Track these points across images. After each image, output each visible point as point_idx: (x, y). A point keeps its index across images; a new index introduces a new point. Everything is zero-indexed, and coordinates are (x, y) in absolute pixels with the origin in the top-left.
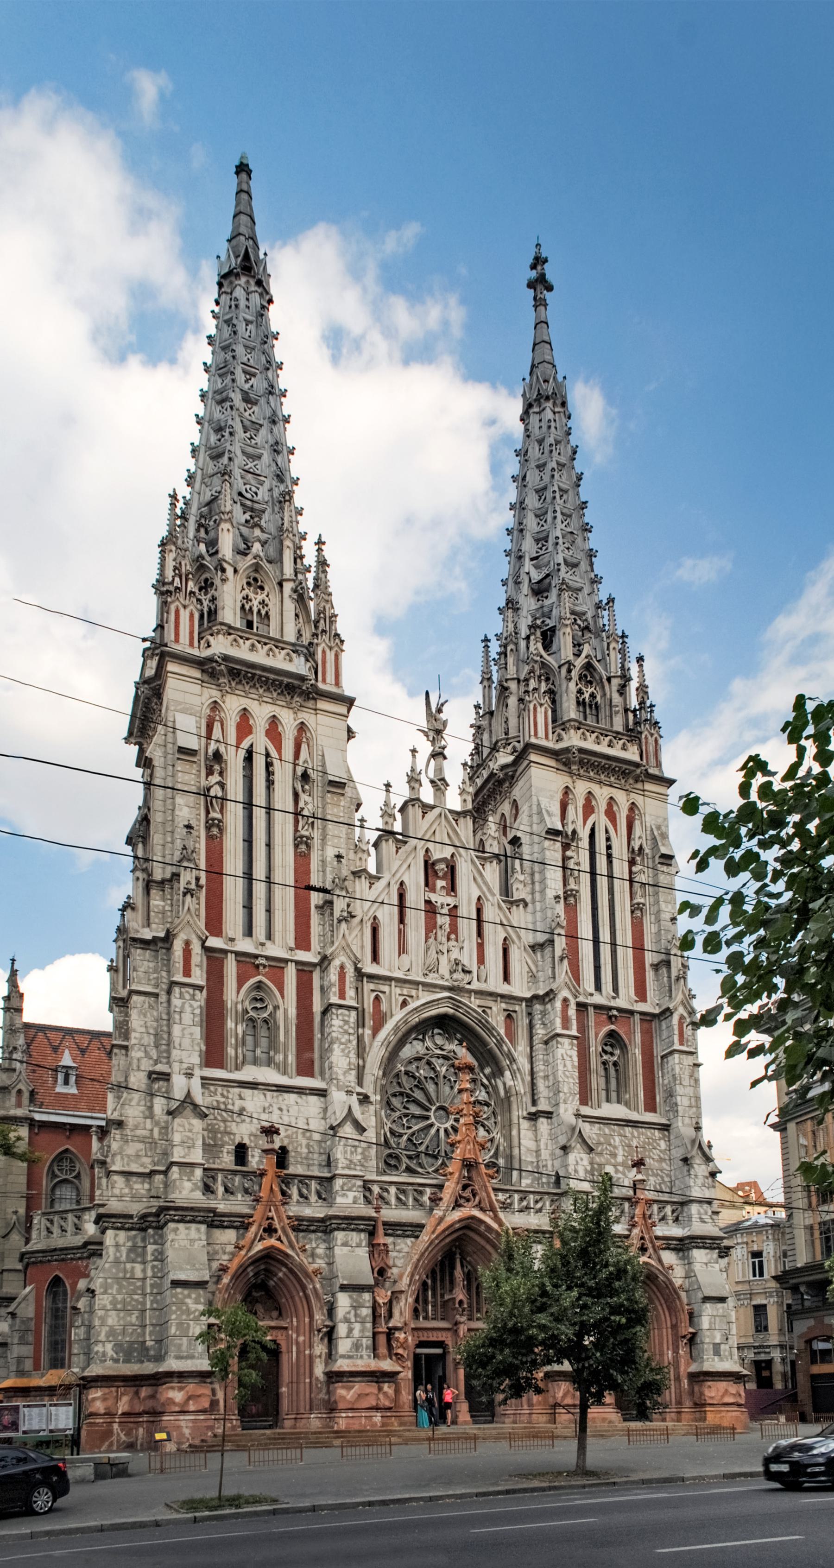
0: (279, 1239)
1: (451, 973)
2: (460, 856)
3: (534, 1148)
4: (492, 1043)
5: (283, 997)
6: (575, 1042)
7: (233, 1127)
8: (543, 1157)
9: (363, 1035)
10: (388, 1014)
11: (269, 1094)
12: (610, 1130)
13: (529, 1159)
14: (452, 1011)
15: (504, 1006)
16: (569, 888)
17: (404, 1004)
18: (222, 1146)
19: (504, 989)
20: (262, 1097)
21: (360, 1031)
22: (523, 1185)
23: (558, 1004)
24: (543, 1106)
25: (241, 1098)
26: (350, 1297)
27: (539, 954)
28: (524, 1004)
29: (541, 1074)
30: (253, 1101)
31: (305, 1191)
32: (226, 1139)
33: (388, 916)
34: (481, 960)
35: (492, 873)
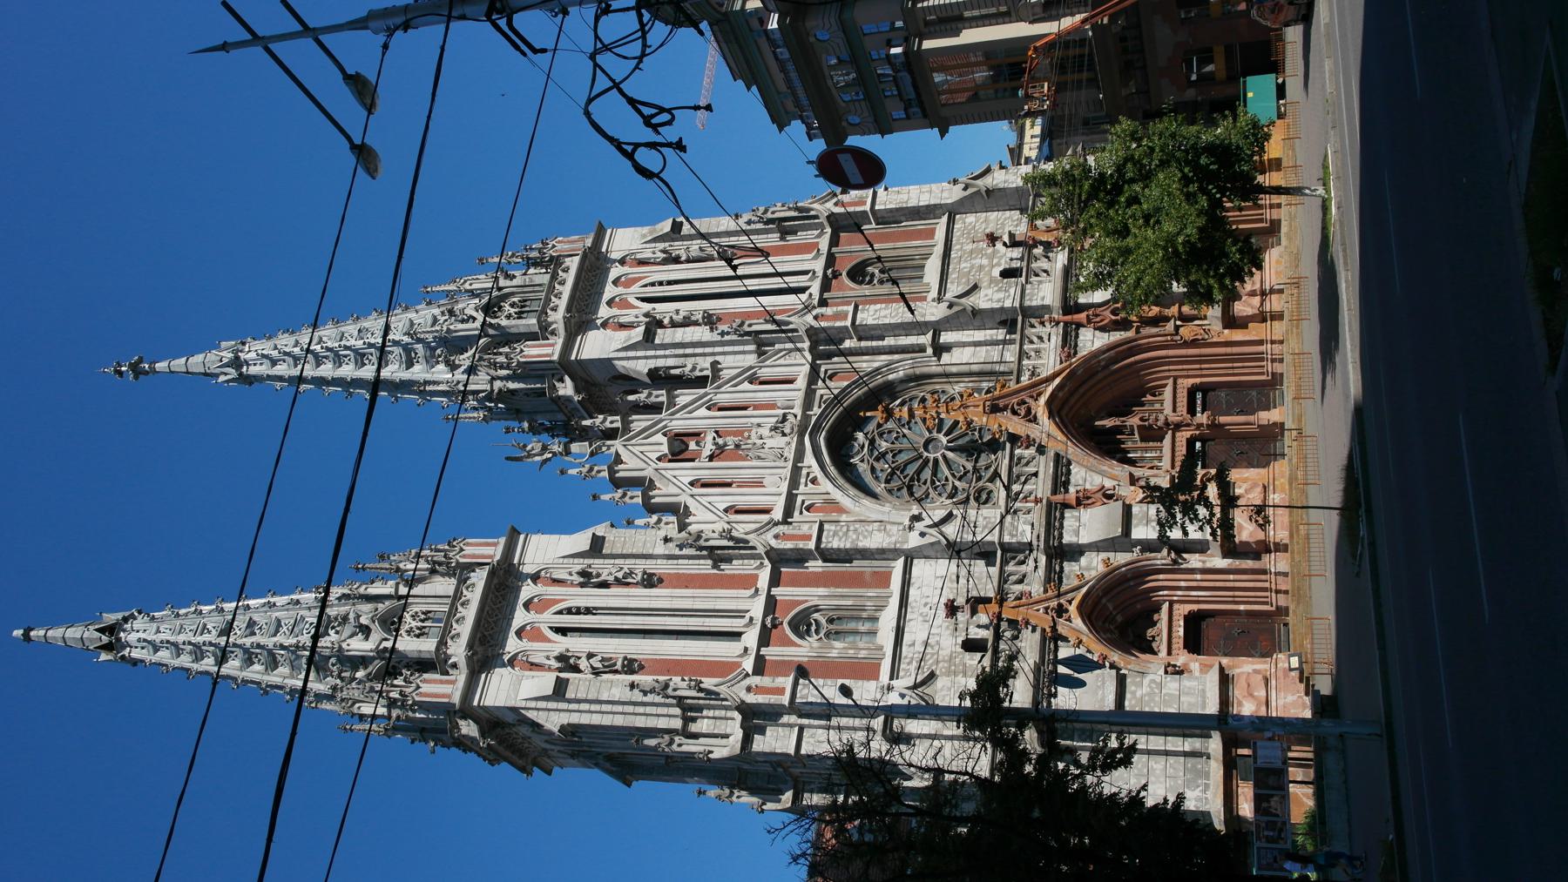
0: (1070, 602)
1: (784, 434)
7: (944, 653)
10: (826, 497)
14: (824, 433)
16: (701, 321)
17: (814, 481)
18: (965, 665)
19: (801, 383)
22: (1012, 359)
24: (926, 339)
25: (914, 644)
26: (1137, 526)
30: (915, 632)
33: (721, 498)
34: (773, 406)
35: (685, 396)
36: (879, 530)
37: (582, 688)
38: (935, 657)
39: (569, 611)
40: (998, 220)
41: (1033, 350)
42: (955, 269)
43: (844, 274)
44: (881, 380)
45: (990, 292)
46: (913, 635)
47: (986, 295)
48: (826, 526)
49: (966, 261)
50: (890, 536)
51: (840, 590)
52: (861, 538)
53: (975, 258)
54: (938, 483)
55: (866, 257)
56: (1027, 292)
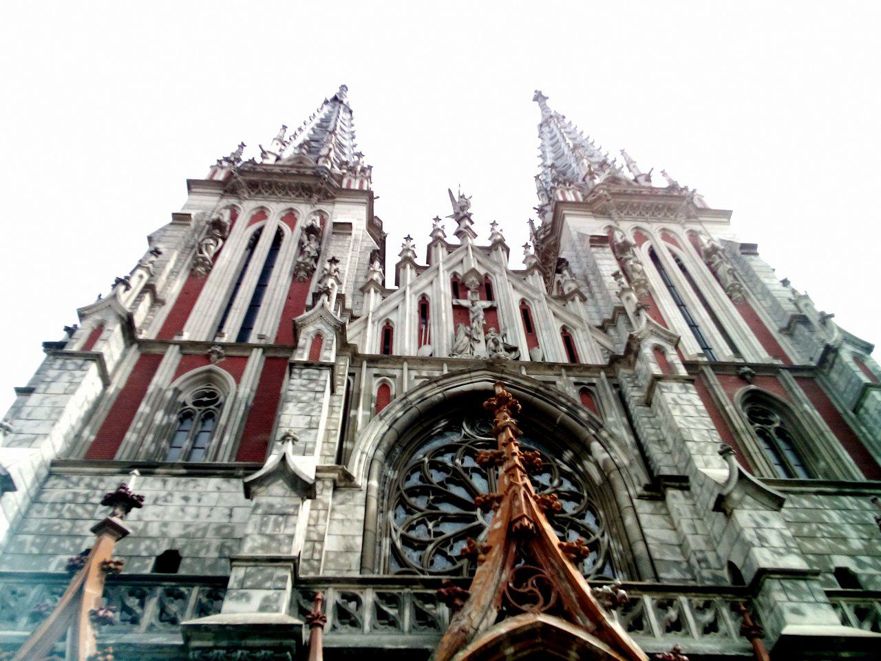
2: (494, 274)
4: (562, 413)
5: (238, 381)
6: (690, 385)
8: (693, 546)
9: (355, 417)
11: (172, 481)
12: (810, 500)
13: (669, 557)
15: (573, 379)
21: (352, 413)
23: (647, 351)
27: (611, 331)
28: (603, 374)
31: (173, 608)
32: (66, 544)
36: (310, 422)
37: (175, 233)
38: (86, 516)
41: (681, 615)
42: (821, 503)
43: (753, 387)
44: (587, 434)
45: (777, 524)
47: (766, 519)
48: (326, 374)
51: (243, 408)
52: (301, 405)
53: (857, 530)
54: (431, 525)
55: (791, 405)
56: (803, 584)
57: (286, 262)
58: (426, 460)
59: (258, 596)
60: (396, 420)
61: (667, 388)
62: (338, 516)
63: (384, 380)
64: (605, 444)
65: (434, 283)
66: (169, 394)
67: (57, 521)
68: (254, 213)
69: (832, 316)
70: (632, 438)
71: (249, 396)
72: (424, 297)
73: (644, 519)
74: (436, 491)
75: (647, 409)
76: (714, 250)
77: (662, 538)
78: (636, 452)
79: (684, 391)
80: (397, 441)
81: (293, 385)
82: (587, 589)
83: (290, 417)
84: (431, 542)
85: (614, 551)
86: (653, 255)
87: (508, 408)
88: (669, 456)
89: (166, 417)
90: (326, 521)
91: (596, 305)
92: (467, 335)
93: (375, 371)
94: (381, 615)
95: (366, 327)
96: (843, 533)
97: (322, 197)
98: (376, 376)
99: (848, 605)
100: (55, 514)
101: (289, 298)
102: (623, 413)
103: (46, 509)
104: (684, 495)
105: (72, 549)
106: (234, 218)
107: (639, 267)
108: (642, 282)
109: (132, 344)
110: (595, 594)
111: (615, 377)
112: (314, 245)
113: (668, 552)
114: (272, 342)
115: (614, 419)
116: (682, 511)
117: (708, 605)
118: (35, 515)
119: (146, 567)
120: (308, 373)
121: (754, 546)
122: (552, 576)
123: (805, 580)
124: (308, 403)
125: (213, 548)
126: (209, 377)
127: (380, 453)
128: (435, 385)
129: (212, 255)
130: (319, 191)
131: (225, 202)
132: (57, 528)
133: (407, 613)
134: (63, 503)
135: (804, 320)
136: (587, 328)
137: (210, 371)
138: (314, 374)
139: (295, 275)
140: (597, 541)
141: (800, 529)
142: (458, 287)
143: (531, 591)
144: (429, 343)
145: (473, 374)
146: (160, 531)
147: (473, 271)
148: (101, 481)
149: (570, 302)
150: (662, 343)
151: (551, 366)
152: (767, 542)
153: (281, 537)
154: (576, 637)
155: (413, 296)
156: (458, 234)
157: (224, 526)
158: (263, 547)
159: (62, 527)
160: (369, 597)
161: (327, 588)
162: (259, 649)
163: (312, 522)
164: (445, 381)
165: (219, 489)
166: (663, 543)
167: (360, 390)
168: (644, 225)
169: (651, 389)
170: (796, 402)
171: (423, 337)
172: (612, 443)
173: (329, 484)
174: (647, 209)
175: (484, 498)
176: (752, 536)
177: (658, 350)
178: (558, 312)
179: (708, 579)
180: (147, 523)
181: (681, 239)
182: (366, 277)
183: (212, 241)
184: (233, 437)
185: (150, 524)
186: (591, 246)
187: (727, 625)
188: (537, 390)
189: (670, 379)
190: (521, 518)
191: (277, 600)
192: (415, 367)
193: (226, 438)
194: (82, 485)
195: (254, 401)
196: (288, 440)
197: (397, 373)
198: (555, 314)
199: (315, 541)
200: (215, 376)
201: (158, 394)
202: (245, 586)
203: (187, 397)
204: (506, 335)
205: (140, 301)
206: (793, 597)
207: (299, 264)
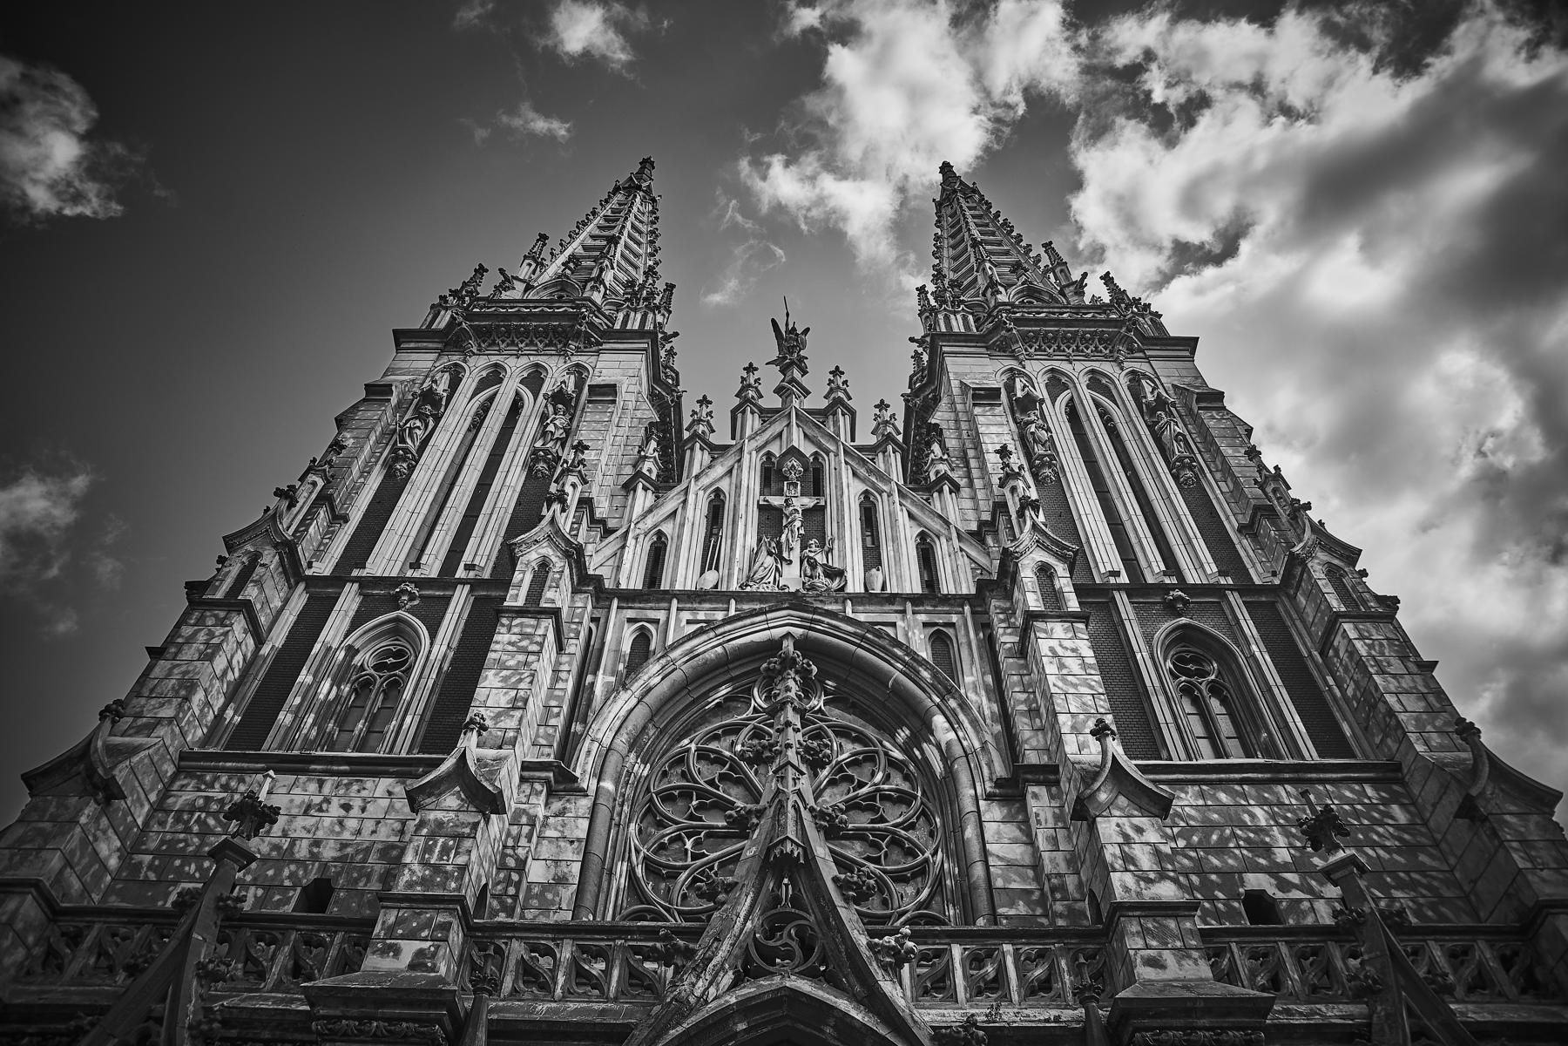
2: (827, 452)
3: (1028, 861)
4: (896, 673)
5: (433, 636)
8: (1048, 868)
9: (593, 684)
11: (330, 782)
15: (923, 618)
20: (313, 787)
21: (589, 678)
23: (1027, 574)
27: (990, 541)
28: (967, 608)
29: (1023, 707)
39: (516, 406)
40: (1423, 873)
42: (1244, 796)
43: (1183, 620)
45: (1152, 836)
46: (284, 790)
48: (547, 624)
49: (1273, 816)
50: (497, 717)
52: (505, 673)
53: (1287, 835)
54: (689, 845)
55: (1235, 648)
56: (1172, 924)
57: (521, 449)
58: (693, 747)
59: (409, 948)
60: (650, 689)
61: (1045, 631)
62: (549, 833)
63: (642, 627)
64: (952, 719)
65: (735, 472)
66: (341, 655)
67: (182, 836)
68: (484, 374)
69: (1308, 506)
70: (995, 707)
71: (445, 656)
72: (718, 492)
73: (990, 830)
74: (702, 794)
75: (1022, 662)
76: (1161, 403)
77: (1010, 856)
78: (998, 728)
79: (1070, 635)
80: (651, 720)
81: (497, 642)
82: (862, 940)
83: (491, 693)
84: (685, 868)
85: (947, 876)
86: (1073, 414)
87: (797, 672)
88: (1039, 733)
89: (335, 688)
90: (529, 841)
91: (974, 498)
92: (770, 554)
93: (630, 614)
94: (580, 975)
95: (623, 547)
96: (1267, 839)
97: (581, 346)
98: (631, 621)
99: (1241, 949)
100: (180, 827)
101: (518, 503)
102: (988, 668)
103: (170, 820)
104: (1049, 791)
105: (197, 875)
106: (454, 384)
107: (1044, 435)
108: (1047, 459)
109: (297, 584)
110: (871, 946)
111: (987, 612)
112: (561, 421)
113: (1014, 877)
114: (486, 575)
115: (972, 678)
116: (1042, 818)
117: (1041, 955)
118: (156, 828)
119: (287, 901)
120: (521, 625)
121: (1115, 870)
122: (818, 923)
123: (1176, 917)
124: (515, 669)
125: (375, 877)
126: (398, 629)
127: (622, 742)
128: (712, 634)
129: (417, 444)
130: (577, 336)
131: (445, 361)
132: (181, 845)
133: (616, 973)
134: (192, 813)
135: (1270, 513)
136: (954, 535)
137: (398, 619)
138: (528, 626)
139: (530, 467)
140: (926, 860)
141: (1208, 836)
142: (772, 475)
143: (786, 945)
144: (717, 569)
145: (770, 616)
146: (310, 852)
147: (793, 452)
148: (242, 781)
149: (936, 495)
150: (1051, 560)
151: (892, 599)
152: (1135, 865)
153: (449, 868)
154: (832, 1008)
155: (701, 493)
156: (779, 390)
157: (392, 846)
158: (424, 881)
159: (187, 845)
160: (566, 952)
161: (510, 938)
162: (400, 1019)
163: (510, 843)
164: (728, 628)
165: (390, 793)
166: (1010, 864)
167: (603, 644)
168: (1065, 367)
169: (1025, 632)
170: (1242, 641)
171: (710, 560)
172: (962, 717)
173: (538, 787)
174: (1068, 341)
175: (738, 812)
176: (1114, 855)
177: (1044, 571)
178: (914, 510)
179: (1061, 916)
180: (294, 841)
181: (1116, 387)
182: (635, 466)
183: (418, 423)
184: (417, 718)
185: (298, 842)
186: (975, 405)
187: (1063, 983)
188: (863, 638)
189: (1052, 617)
190: (782, 842)
191: (434, 955)
192: (689, 605)
193: (408, 719)
194: (217, 786)
195: (451, 665)
196: (472, 730)
197: (661, 615)
198: (911, 516)
199: (512, 869)
200: (402, 625)
201: (325, 656)
202: (394, 935)
203: (365, 658)
204: (831, 550)
205: (312, 519)
206: (1154, 943)
207: (535, 451)
